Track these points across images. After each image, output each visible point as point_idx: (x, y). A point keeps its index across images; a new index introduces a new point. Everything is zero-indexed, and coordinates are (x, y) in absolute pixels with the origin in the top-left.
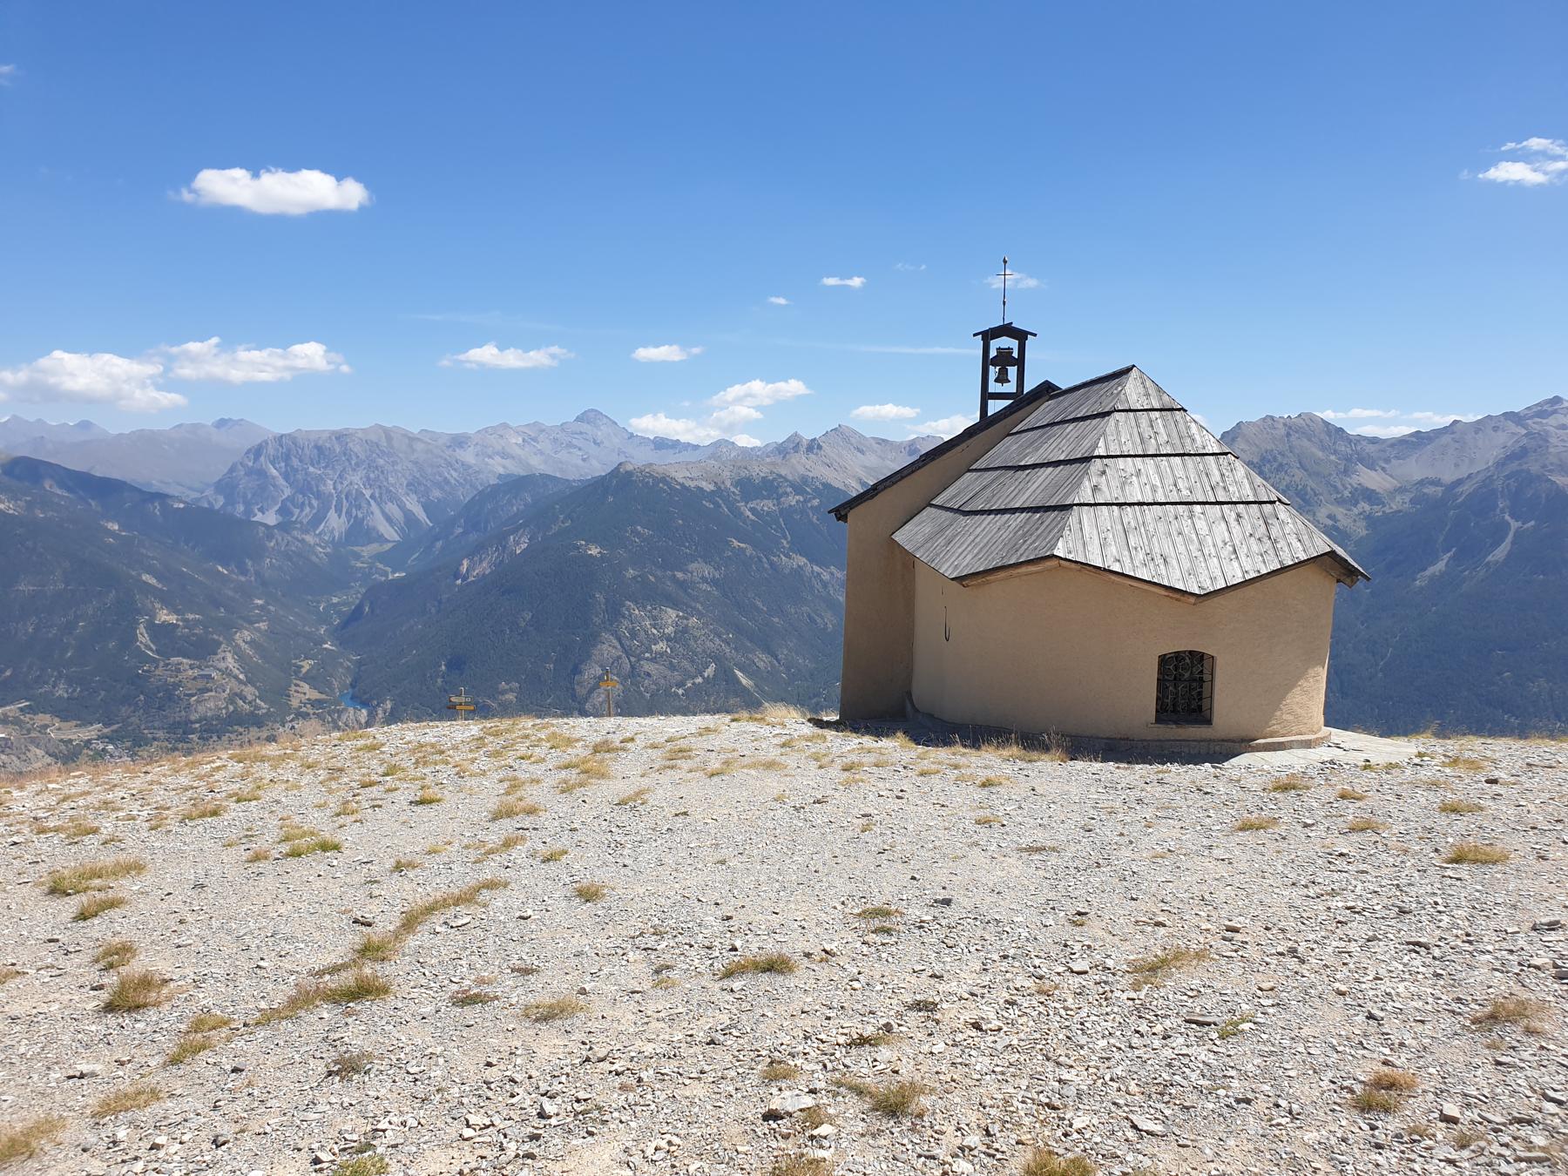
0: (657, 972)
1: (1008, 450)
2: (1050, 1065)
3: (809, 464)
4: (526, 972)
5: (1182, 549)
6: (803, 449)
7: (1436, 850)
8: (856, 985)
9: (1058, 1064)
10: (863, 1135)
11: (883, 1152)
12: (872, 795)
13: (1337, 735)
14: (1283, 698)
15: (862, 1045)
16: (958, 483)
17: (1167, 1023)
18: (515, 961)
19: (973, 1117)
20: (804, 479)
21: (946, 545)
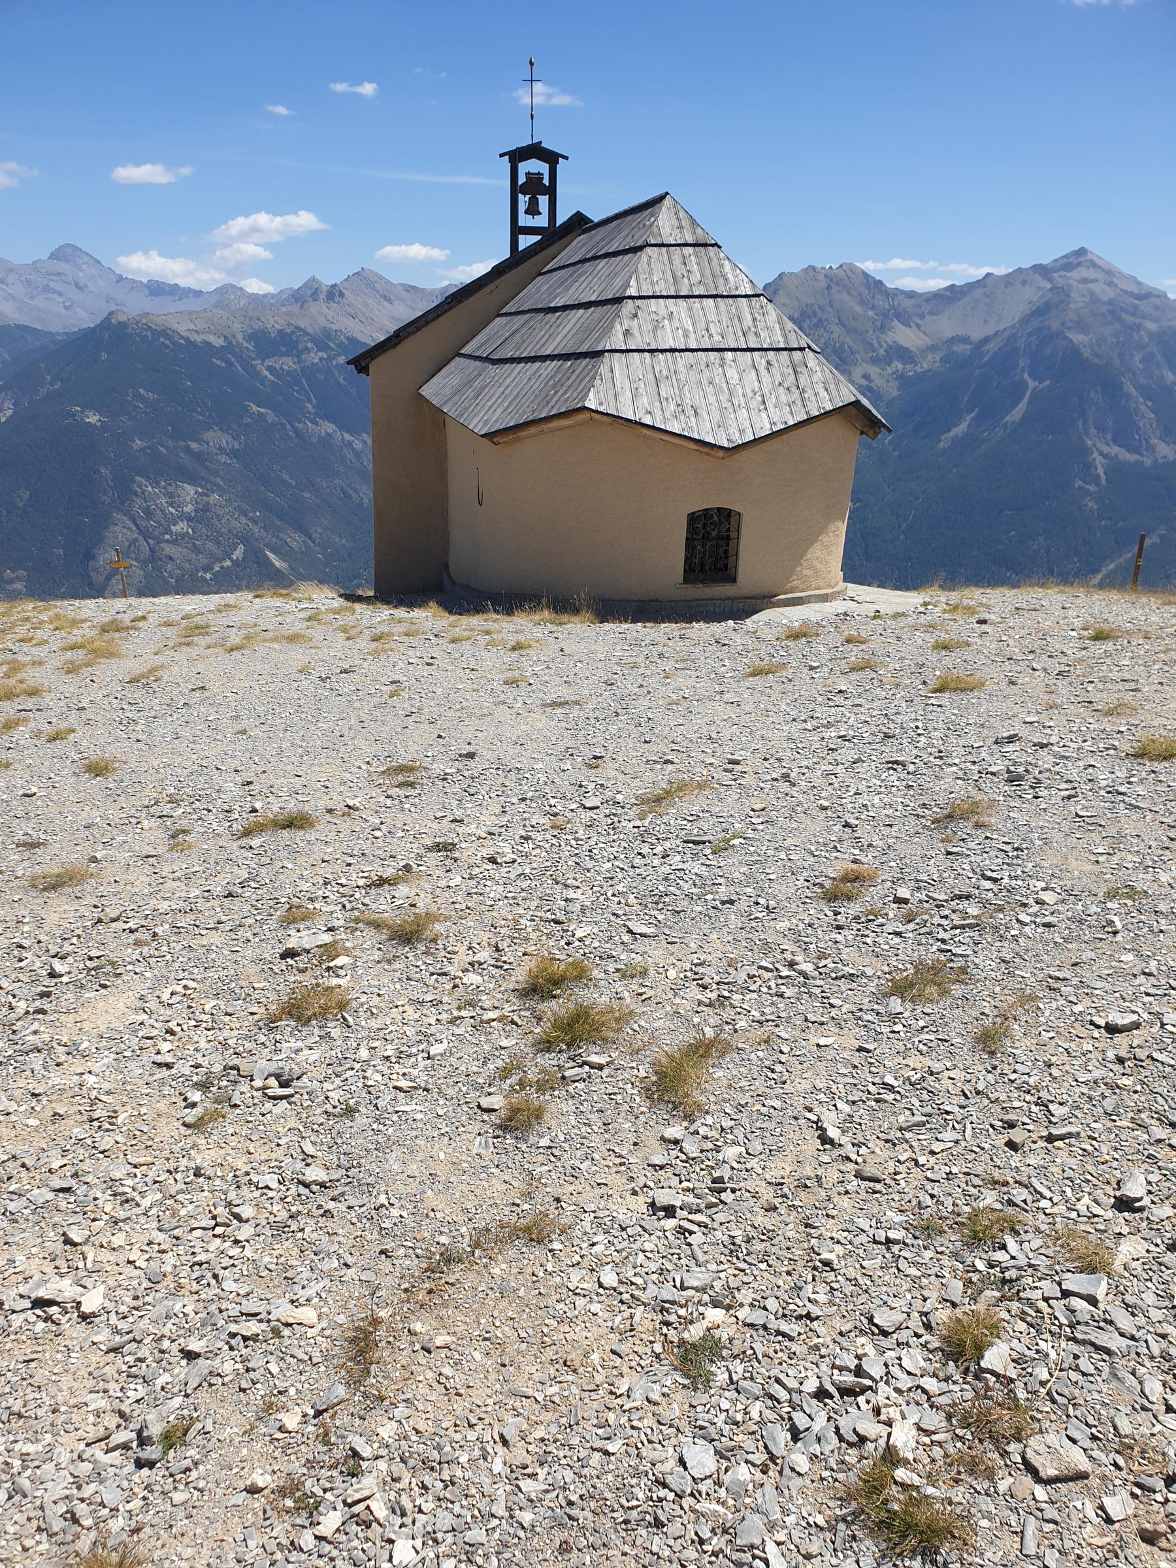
0: (173, 837)
1: (539, 291)
2: (559, 888)
3: (331, 314)
4: (32, 845)
5: (712, 399)
6: (322, 296)
7: (924, 683)
8: (377, 834)
9: (566, 886)
10: (379, 962)
11: (397, 974)
12: (401, 662)
13: (853, 589)
14: (804, 553)
15: (380, 885)
16: (488, 330)
17: (667, 845)
18: (19, 836)
19: (485, 937)
20: (327, 333)
21: (478, 398)
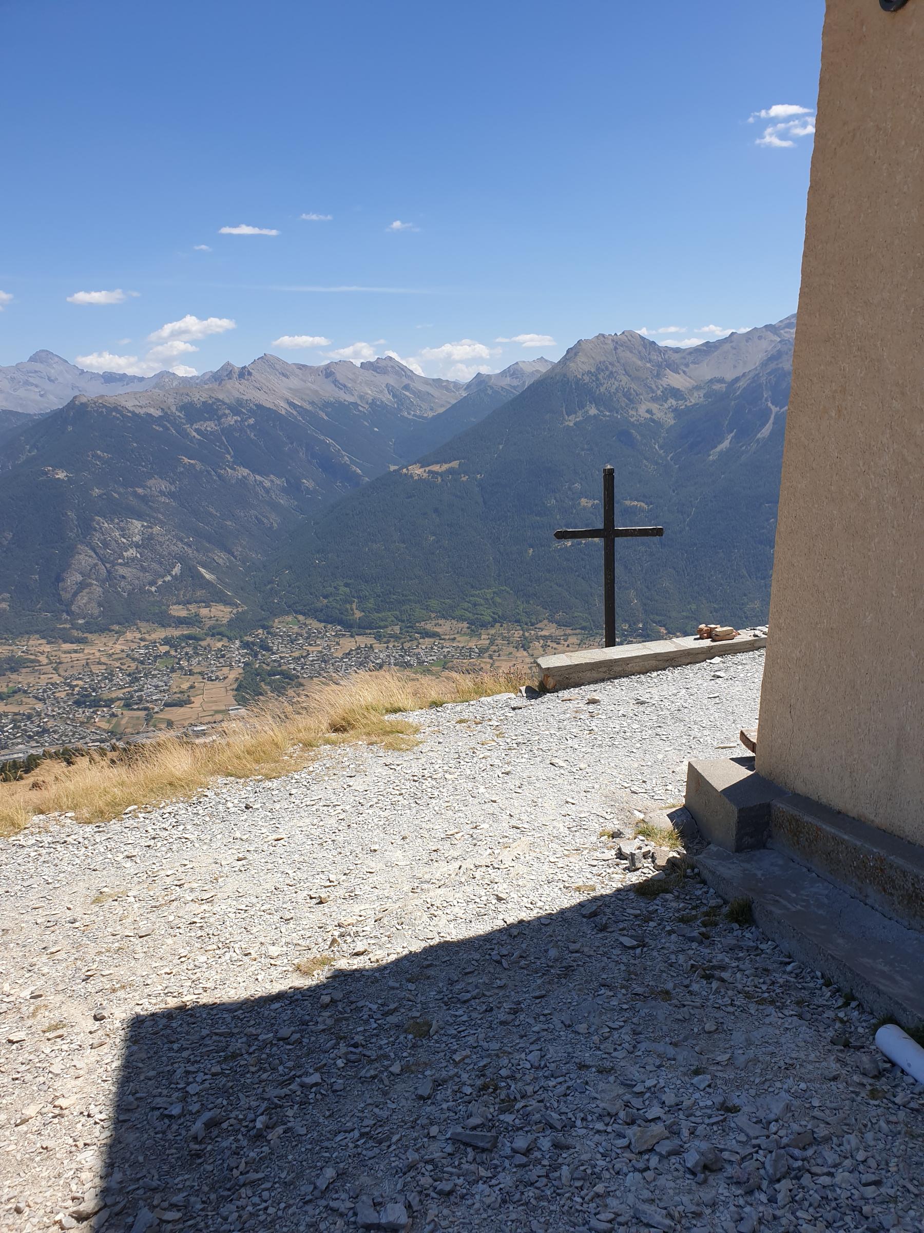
6: (235, 375)
20: (240, 402)
